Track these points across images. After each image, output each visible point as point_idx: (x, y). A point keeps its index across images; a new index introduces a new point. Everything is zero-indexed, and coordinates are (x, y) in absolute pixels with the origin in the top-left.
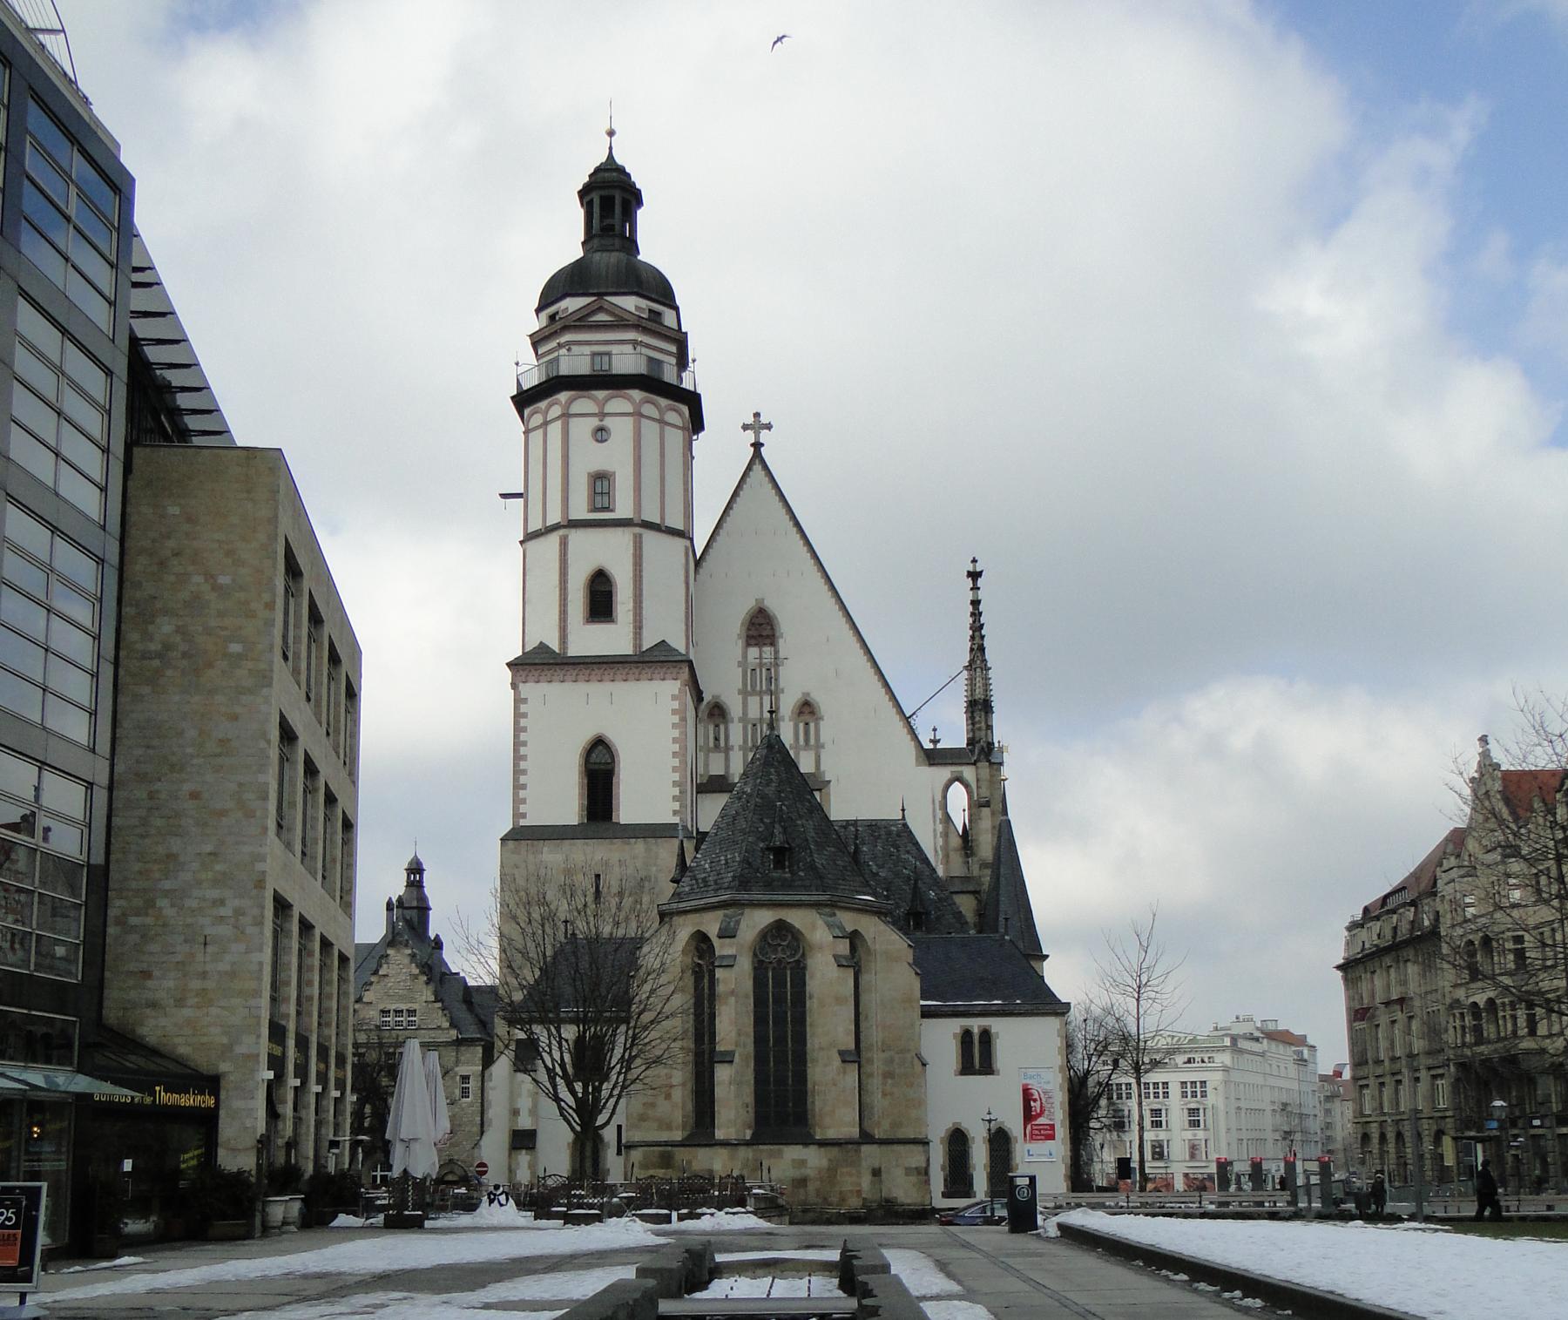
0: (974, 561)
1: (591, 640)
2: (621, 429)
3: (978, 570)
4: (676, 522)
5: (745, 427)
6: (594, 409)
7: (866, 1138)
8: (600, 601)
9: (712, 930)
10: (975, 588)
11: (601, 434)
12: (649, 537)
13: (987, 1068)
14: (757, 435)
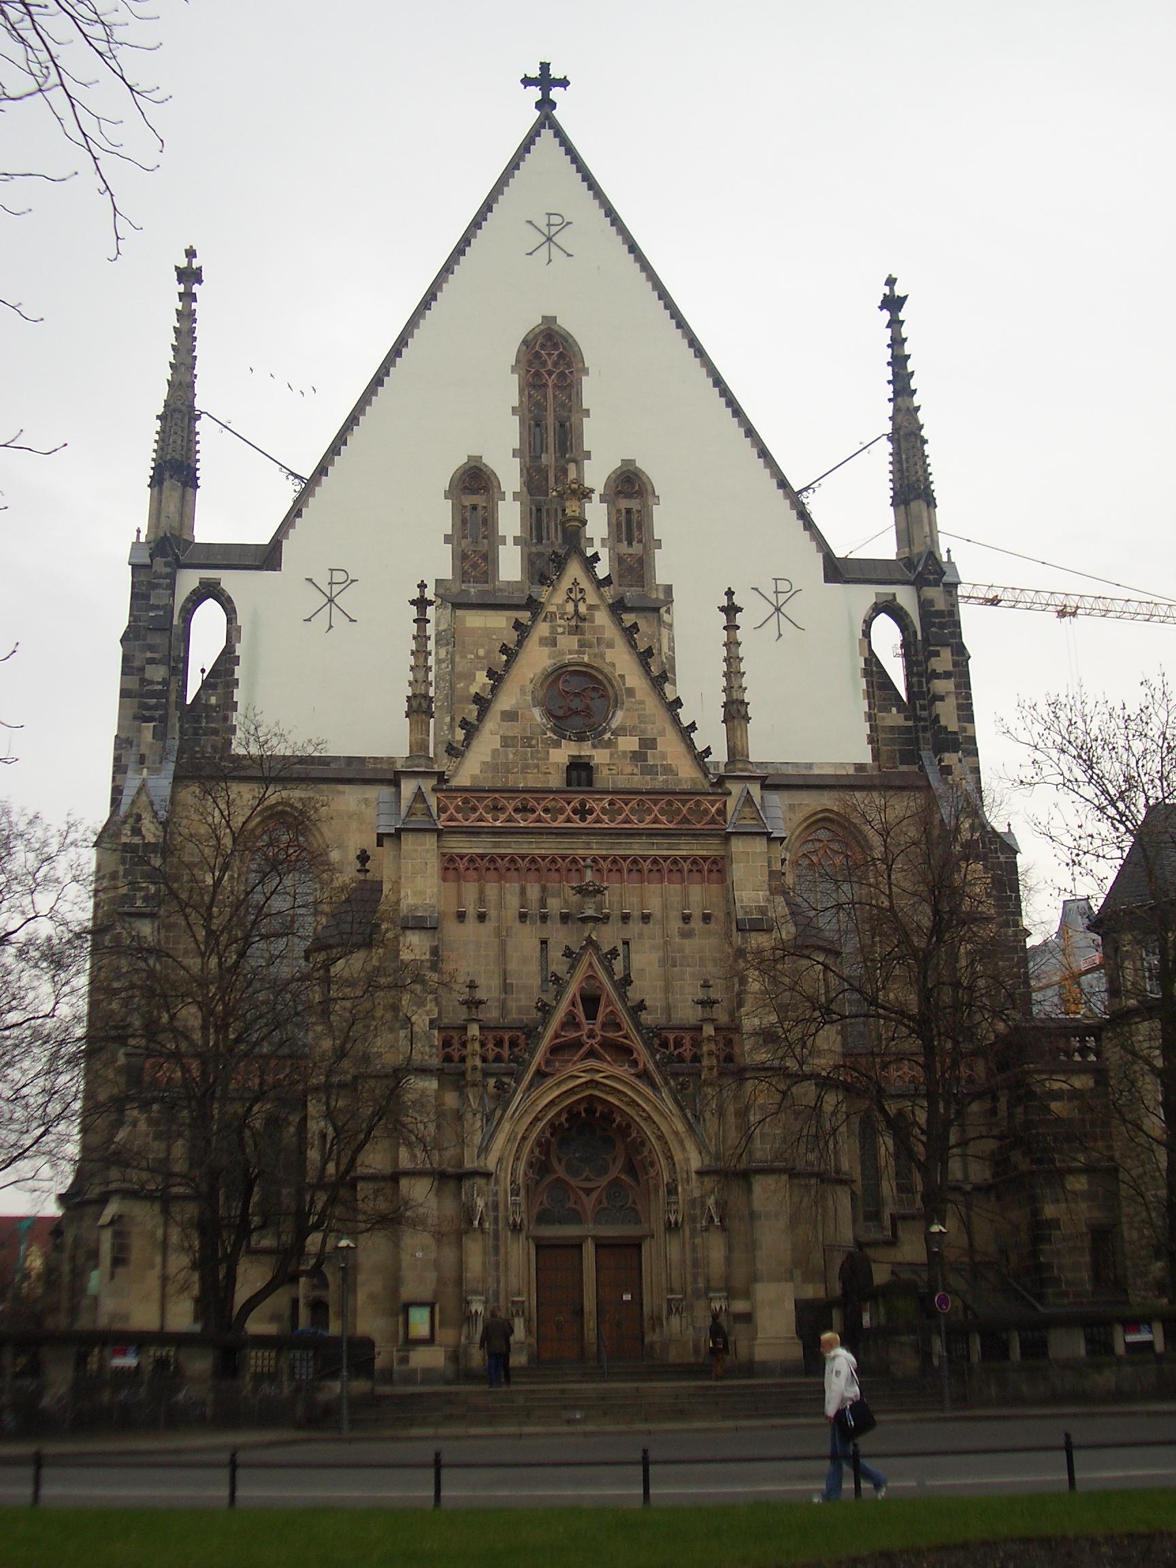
0: (891, 282)
3: (899, 291)
5: (527, 81)
10: (895, 324)
14: (546, 93)
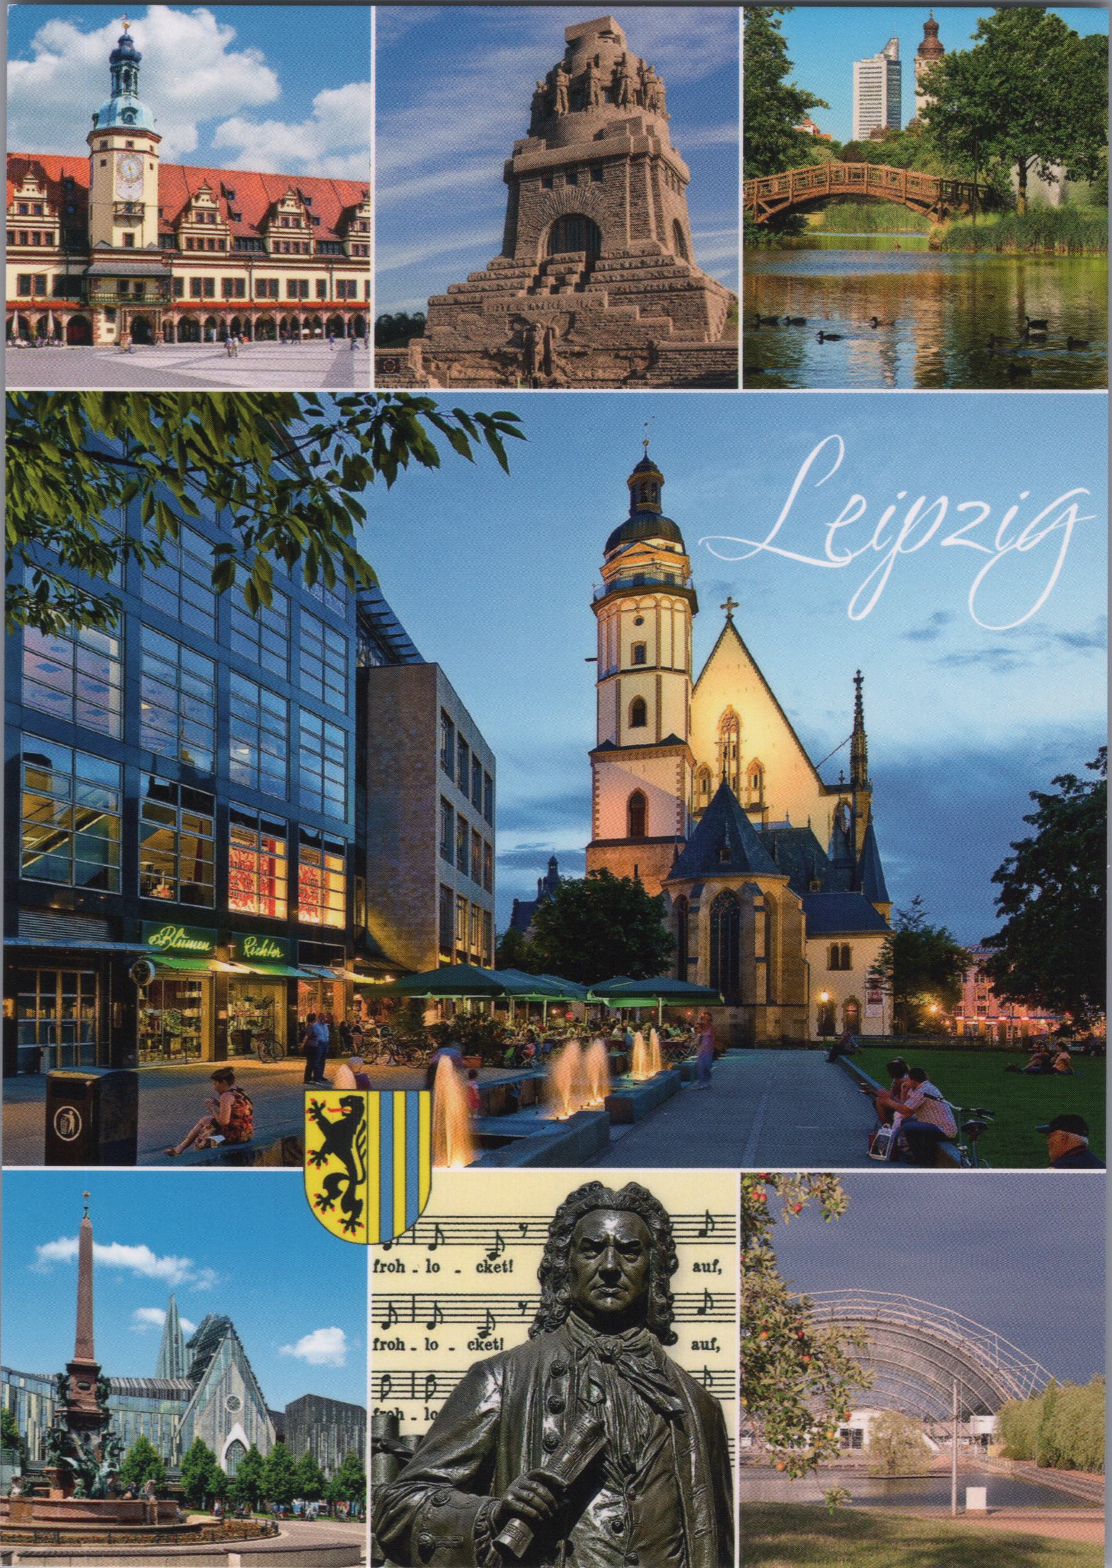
1: (632, 736)
2: (649, 616)
4: (680, 664)
5: (722, 607)
6: (633, 606)
7: (771, 1002)
8: (639, 716)
9: (688, 894)
11: (639, 622)
12: (666, 677)
13: (846, 966)
